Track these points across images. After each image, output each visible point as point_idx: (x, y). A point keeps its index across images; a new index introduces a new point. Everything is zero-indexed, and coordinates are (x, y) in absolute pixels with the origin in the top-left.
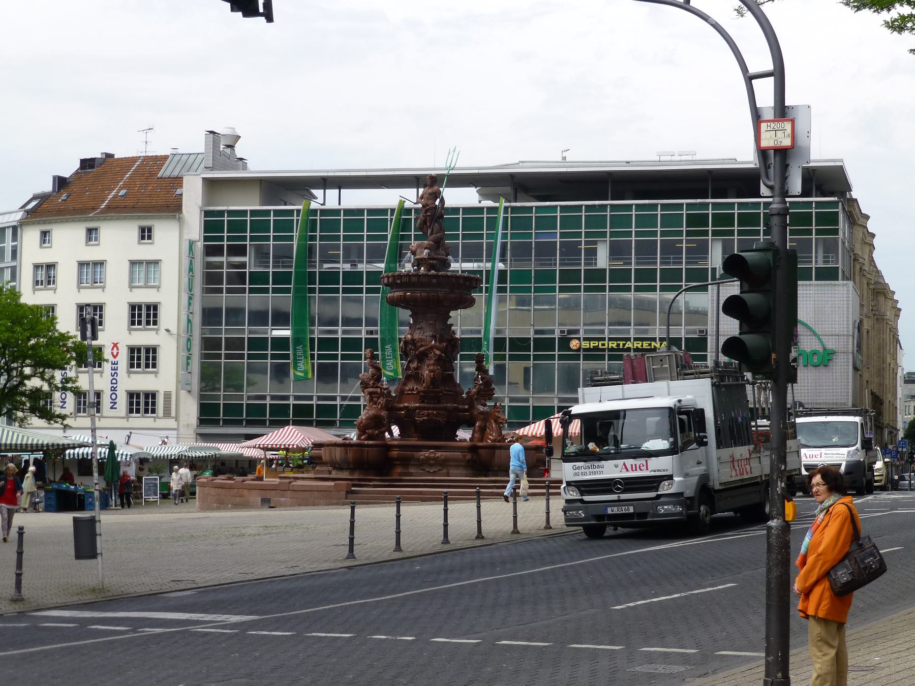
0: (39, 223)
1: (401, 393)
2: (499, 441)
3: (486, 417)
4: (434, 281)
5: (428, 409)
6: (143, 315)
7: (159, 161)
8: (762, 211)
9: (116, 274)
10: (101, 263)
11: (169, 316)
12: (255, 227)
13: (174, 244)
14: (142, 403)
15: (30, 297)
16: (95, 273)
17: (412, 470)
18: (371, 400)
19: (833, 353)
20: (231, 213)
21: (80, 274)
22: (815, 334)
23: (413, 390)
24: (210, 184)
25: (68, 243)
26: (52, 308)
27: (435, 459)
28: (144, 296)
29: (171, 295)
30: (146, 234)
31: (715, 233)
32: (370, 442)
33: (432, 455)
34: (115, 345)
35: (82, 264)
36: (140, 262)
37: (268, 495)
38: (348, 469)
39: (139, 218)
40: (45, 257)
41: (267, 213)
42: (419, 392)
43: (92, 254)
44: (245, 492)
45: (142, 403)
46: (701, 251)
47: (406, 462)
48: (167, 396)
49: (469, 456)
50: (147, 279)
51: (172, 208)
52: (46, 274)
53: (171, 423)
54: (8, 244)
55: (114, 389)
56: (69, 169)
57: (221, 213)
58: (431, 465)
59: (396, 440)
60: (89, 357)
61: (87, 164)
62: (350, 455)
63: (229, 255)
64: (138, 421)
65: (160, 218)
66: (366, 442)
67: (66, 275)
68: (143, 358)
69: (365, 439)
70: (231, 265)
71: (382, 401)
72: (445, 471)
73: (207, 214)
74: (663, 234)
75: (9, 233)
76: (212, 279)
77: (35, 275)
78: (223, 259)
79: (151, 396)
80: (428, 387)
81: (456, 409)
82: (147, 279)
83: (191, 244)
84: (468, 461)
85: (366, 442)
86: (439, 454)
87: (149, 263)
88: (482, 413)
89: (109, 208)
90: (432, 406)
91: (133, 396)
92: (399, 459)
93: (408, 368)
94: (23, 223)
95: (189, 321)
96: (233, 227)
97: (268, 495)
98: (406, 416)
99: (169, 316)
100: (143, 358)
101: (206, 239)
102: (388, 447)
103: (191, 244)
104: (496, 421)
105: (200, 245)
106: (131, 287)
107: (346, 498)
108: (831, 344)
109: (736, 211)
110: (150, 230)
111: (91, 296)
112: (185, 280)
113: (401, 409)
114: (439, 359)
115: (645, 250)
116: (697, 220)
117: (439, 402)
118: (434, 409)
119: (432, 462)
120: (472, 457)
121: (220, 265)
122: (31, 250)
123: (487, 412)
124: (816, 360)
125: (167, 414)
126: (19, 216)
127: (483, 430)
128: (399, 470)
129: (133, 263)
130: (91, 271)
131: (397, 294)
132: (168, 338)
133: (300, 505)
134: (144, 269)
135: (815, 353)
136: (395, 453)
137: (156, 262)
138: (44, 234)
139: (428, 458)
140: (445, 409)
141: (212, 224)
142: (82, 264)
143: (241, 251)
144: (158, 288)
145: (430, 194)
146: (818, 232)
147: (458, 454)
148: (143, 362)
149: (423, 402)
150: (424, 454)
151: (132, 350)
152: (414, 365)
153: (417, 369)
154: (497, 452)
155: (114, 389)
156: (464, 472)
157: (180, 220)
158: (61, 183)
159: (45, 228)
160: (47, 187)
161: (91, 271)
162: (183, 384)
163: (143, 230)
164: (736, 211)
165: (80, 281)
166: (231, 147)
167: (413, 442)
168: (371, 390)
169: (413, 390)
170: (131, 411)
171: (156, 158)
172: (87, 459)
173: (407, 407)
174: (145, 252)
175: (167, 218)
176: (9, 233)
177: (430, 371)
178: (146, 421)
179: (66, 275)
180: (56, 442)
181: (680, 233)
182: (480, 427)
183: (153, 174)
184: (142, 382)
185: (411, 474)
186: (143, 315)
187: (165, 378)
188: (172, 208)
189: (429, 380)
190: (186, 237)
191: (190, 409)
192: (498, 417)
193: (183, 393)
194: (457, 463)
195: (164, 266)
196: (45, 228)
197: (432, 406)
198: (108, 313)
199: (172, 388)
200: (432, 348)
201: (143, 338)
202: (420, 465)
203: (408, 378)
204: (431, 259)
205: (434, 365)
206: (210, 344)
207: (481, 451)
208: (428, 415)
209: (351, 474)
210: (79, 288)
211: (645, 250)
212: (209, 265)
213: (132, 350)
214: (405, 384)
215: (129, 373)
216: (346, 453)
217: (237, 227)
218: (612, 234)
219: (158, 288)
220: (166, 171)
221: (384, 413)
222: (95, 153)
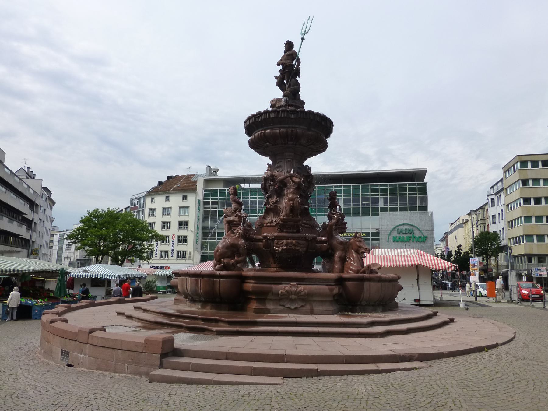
0: (151, 195)
1: (261, 225)
2: (364, 272)
3: (346, 246)
4: (293, 116)
5: (286, 238)
6: (183, 225)
7: (192, 176)
9: (175, 211)
10: (170, 208)
11: (192, 225)
12: (221, 195)
13: (193, 201)
14: (182, 255)
15: (148, 219)
16: (168, 211)
17: (270, 306)
18: (229, 229)
19: (426, 237)
20: (213, 190)
21: (163, 211)
22: (420, 230)
23: (272, 222)
24: (207, 181)
25: (160, 202)
26: (153, 223)
27: (298, 293)
28: (183, 219)
29: (192, 218)
30: (185, 198)
31: (381, 195)
32: (223, 273)
33: (294, 289)
34: (174, 235)
35: (164, 208)
36: (183, 207)
37: (70, 346)
38: (200, 301)
39: (183, 193)
40: (153, 206)
41: (225, 190)
42: (277, 224)
43: (167, 205)
45: (182, 255)
46: (375, 201)
47: (262, 296)
48: (190, 252)
49: (336, 290)
50: (185, 213)
51: (193, 189)
52: (153, 211)
53: (191, 262)
54: (142, 203)
55: (173, 250)
56: (164, 179)
57: (209, 190)
58: (292, 301)
59: (257, 270)
60: (164, 239)
61: (170, 178)
62: (201, 288)
63: (212, 204)
64: (180, 261)
65: (190, 192)
66: (218, 273)
67: (159, 212)
68: (183, 239)
69: (221, 269)
70: (212, 208)
71: (240, 229)
72: (308, 307)
73: (205, 191)
74: (362, 195)
75: (142, 199)
76: (206, 212)
77: (149, 212)
78: (210, 206)
79: (185, 252)
80: (287, 215)
81: (314, 238)
82: (185, 213)
83: (199, 201)
84: (334, 296)
85: (218, 273)
86: (301, 287)
87: (186, 207)
88: (341, 243)
89: (173, 190)
90: (290, 235)
91: (179, 252)
92: (254, 292)
93: (267, 203)
94: (146, 196)
95: (198, 227)
96: (214, 195)
98: (264, 246)
99: (192, 225)
100: (183, 239)
101: (204, 199)
102: (243, 279)
103: (199, 201)
104: (357, 252)
105: (202, 201)
106: (179, 216)
107: (161, 366)
108: (426, 234)
109: (388, 187)
110: (186, 196)
111: (166, 219)
112: (197, 213)
113: (260, 240)
114: (298, 188)
115: (356, 201)
116: (375, 191)
117: (298, 232)
118: (293, 238)
119: (293, 297)
120: (339, 289)
121: (209, 208)
122: (149, 204)
123: (347, 243)
124: (420, 240)
125: (190, 259)
126: (145, 193)
127: (343, 260)
128: (254, 305)
129: (180, 208)
130: (167, 211)
131: (257, 134)
132: (190, 233)
133: (98, 369)
134: (184, 209)
135: (420, 237)
136: (249, 286)
137: (188, 207)
138: (153, 199)
139: (289, 293)
140: (305, 238)
141: (206, 194)
142: (164, 208)
143: (215, 203)
144: (188, 216)
145: (288, 55)
146: (419, 194)
147: (324, 288)
148: (182, 241)
149: (282, 231)
150: (283, 288)
151: (179, 237)
152: (274, 200)
153: (276, 202)
154: (366, 284)
155: (173, 250)
156: (331, 308)
157: (196, 193)
158: (160, 183)
159: (153, 197)
160: (156, 184)
161: (167, 211)
162: (195, 248)
163: (184, 196)
164: (388, 187)
165: (163, 214)
166: (216, 172)
167: (272, 272)
168: (229, 219)
169: (272, 222)
170: (178, 258)
171: (191, 175)
172: (97, 277)
173: (265, 237)
174: (184, 204)
175: (192, 192)
176: (142, 199)
177: (290, 200)
178: (183, 261)
179: (159, 212)
180: (16, 269)
181: (368, 195)
182: (340, 257)
183: (189, 180)
184: (182, 248)
185: (268, 311)
186: (183, 225)
187: (189, 247)
188: (193, 189)
189: (288, 208)
190: (198, 198)
191: (198, 257)
192: (360, 247)
193: (195, 251)
194: (322, 299)
195: (190, 208)
196: (153, 197)
197: (290, 235)
198: (171, 224)
199: (192, 250)
200: (291, 176)
201: (183, 233)
202: (280, 300)
203: (268, 212)
204: (289, 105)
205: (293, 193)
206: (205, 235)
207: (348, 284)
208: (286, 245)
209: (203, 307)
210: (163, 216)
211: (356, 201)
212: (205, 208)
213: (179, 237)
214: (264, 218)
215: (178, 245)
216: (197, 284)
217: (214, 195)
218: (344, 196)
219: (188, 216)
220: (193, 179)
221: (241, 242)
222: (173, 174)
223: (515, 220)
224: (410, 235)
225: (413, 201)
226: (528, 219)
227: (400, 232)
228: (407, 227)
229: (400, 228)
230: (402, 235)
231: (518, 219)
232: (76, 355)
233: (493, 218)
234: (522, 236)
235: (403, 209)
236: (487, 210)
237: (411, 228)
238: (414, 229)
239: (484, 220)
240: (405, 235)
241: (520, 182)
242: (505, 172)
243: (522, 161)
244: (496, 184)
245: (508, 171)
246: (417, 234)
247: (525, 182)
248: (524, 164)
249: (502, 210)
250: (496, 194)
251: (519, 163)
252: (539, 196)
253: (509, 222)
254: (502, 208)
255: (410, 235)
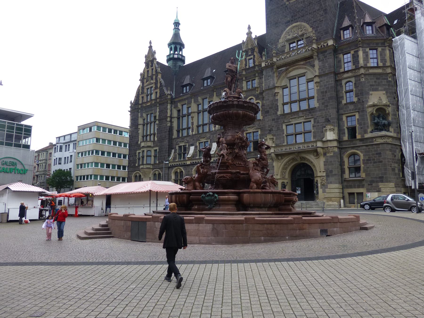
8: (7, 124)
22: (22, 164)
44: (306, 226)
97: (325, 227)
108: (27, 167)
223: (85, 164)
224: (14, 167)
225: (19, 138)
226: (96, 164)
227: (6, 164)
228: (12, 160)
229: (5, 160)
230: (5, 167)
231: (88, 163)
232: (330, 230)
233: (59, 160)
234: (91, 176)
235: (10, 145)
236: (51, 153)
237: (15, 161)
238: (17, 162)
239: (46, 160)
240: (8, 167)
241: (95, 139)
242: (79, 130)
243: (99, 126)
244: (64, 136)
245: (83, 129)
246: (19, 167)
247: (98, 140)
248: (99, 128)
249: (71, 156)
250: (64, 143)
251: (96, 127)
252: (104, 150)
253: (78, 165)
254: (73, 154)
255: (11, 167)
